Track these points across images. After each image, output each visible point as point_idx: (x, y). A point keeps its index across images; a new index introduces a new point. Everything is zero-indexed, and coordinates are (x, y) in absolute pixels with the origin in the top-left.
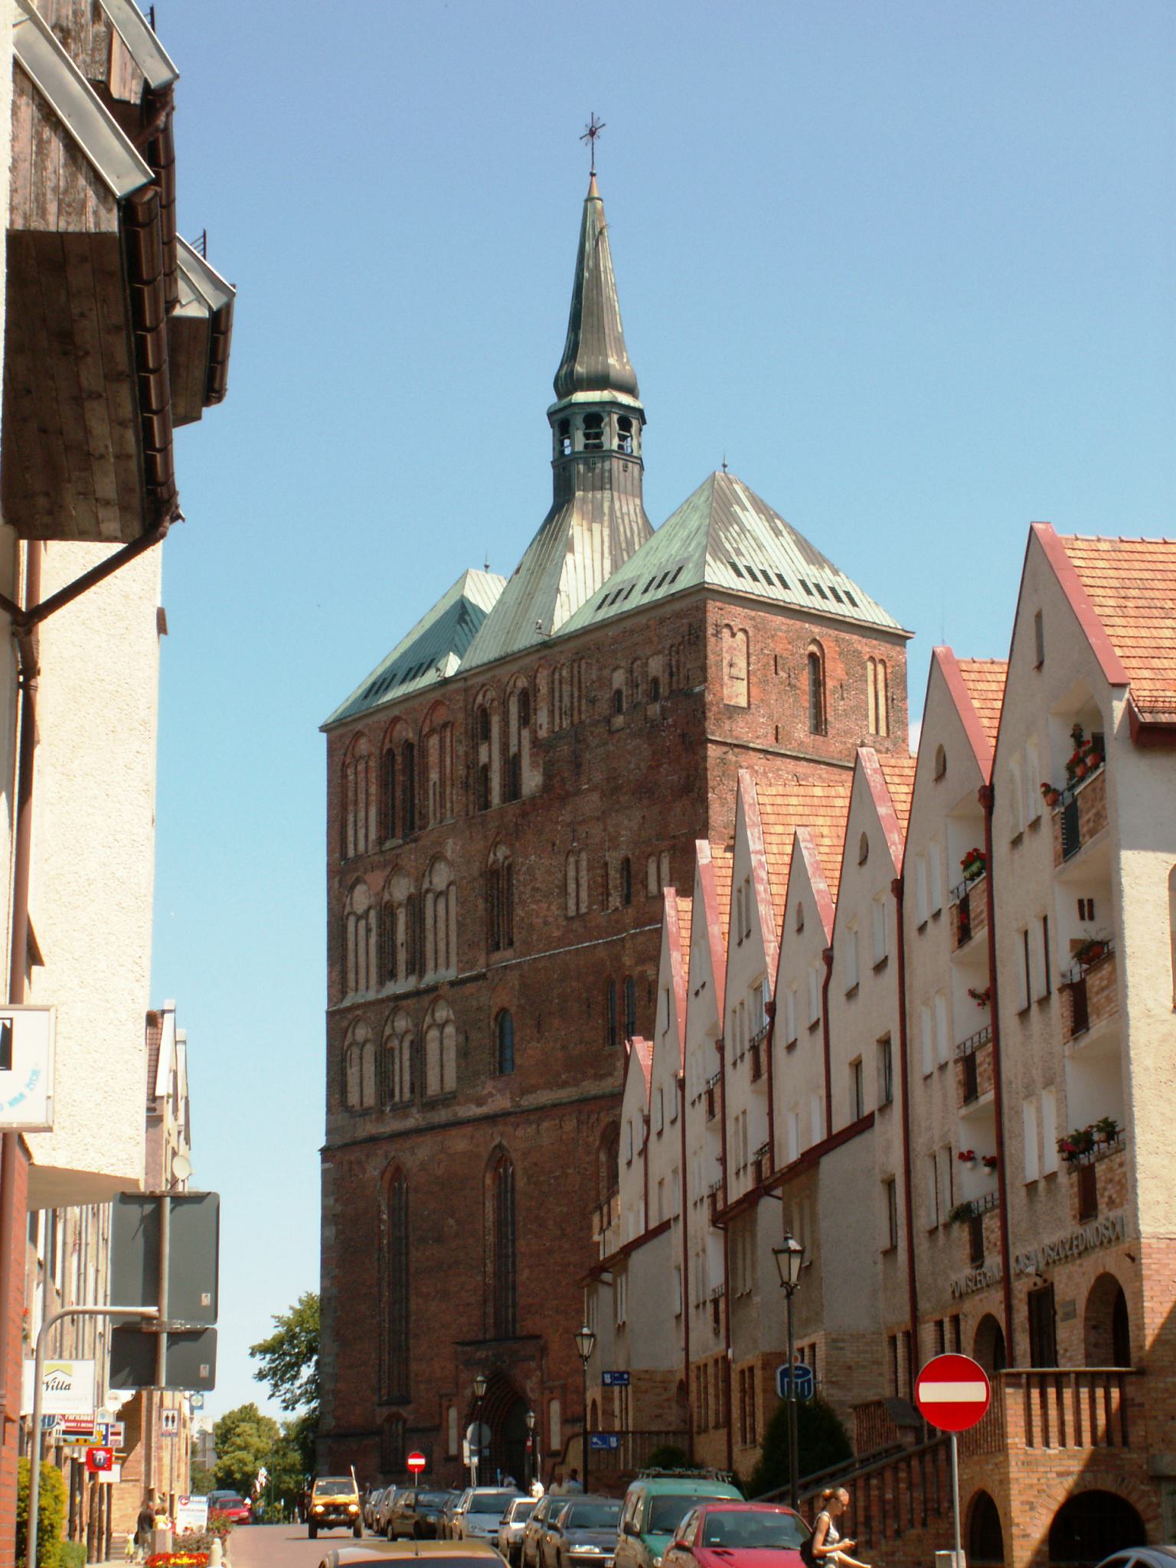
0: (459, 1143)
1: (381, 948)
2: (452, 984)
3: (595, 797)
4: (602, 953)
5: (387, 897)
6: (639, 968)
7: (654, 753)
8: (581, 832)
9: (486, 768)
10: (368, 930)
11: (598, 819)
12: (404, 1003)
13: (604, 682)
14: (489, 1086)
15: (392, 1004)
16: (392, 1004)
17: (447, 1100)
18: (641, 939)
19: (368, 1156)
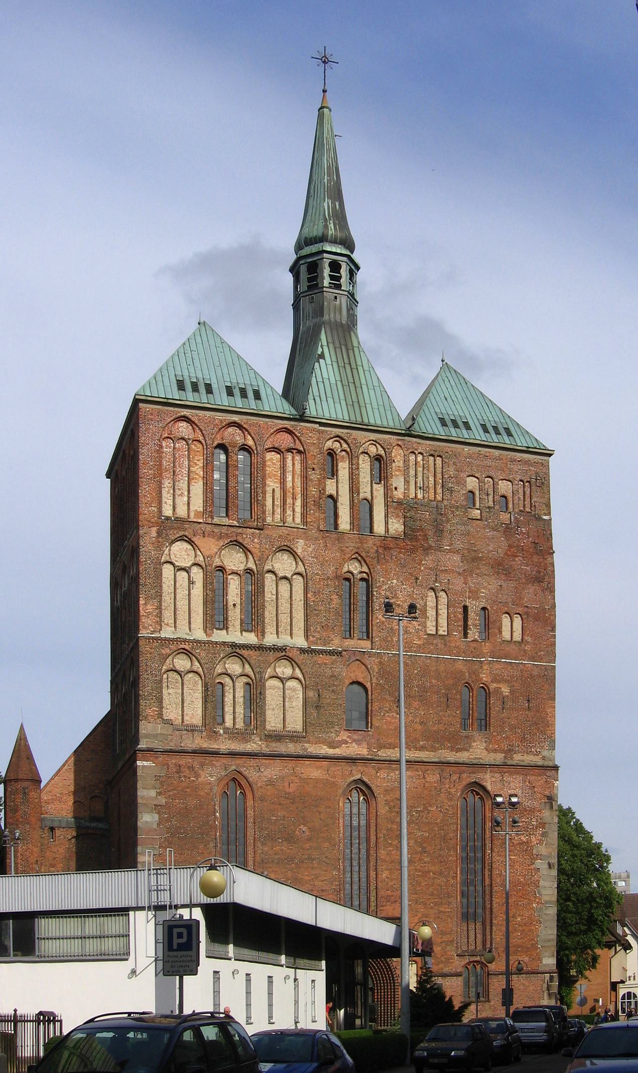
0: (314, 772)
1: (207, 602)
2: (302, 651)
3: (457, 558)
4: (460, 666)
5: (217, 562)
6: (495, 685)
7: (510, 546)
8: (444, 577)
9: (334, 499)
10: (191, 582)
11: (460, 574)
12: (244, 652)
13: (462, 483)
14: (344, 736)
15: (229, 650)
16: (229, 650)
17: (294, 737)
18: (497, 666)
19: (202, 765)
